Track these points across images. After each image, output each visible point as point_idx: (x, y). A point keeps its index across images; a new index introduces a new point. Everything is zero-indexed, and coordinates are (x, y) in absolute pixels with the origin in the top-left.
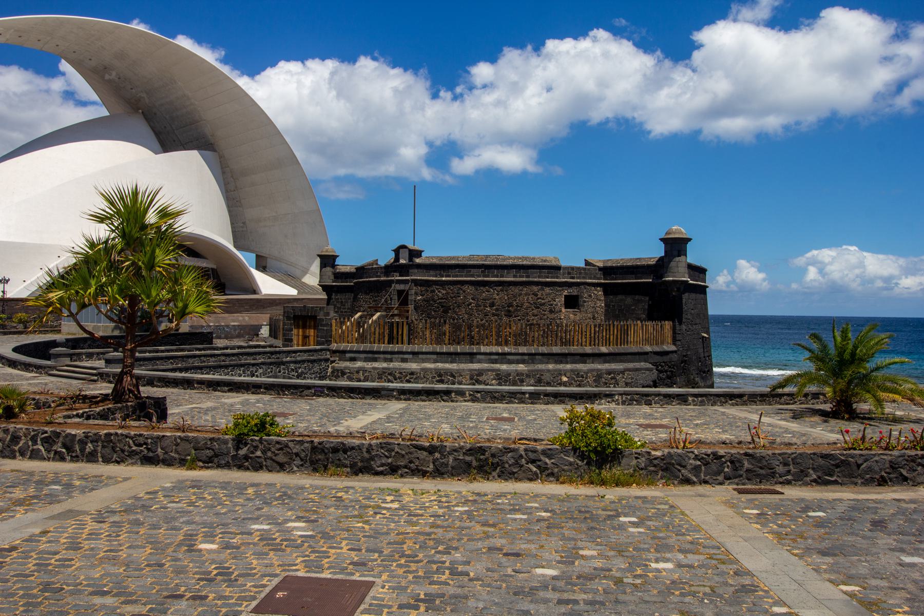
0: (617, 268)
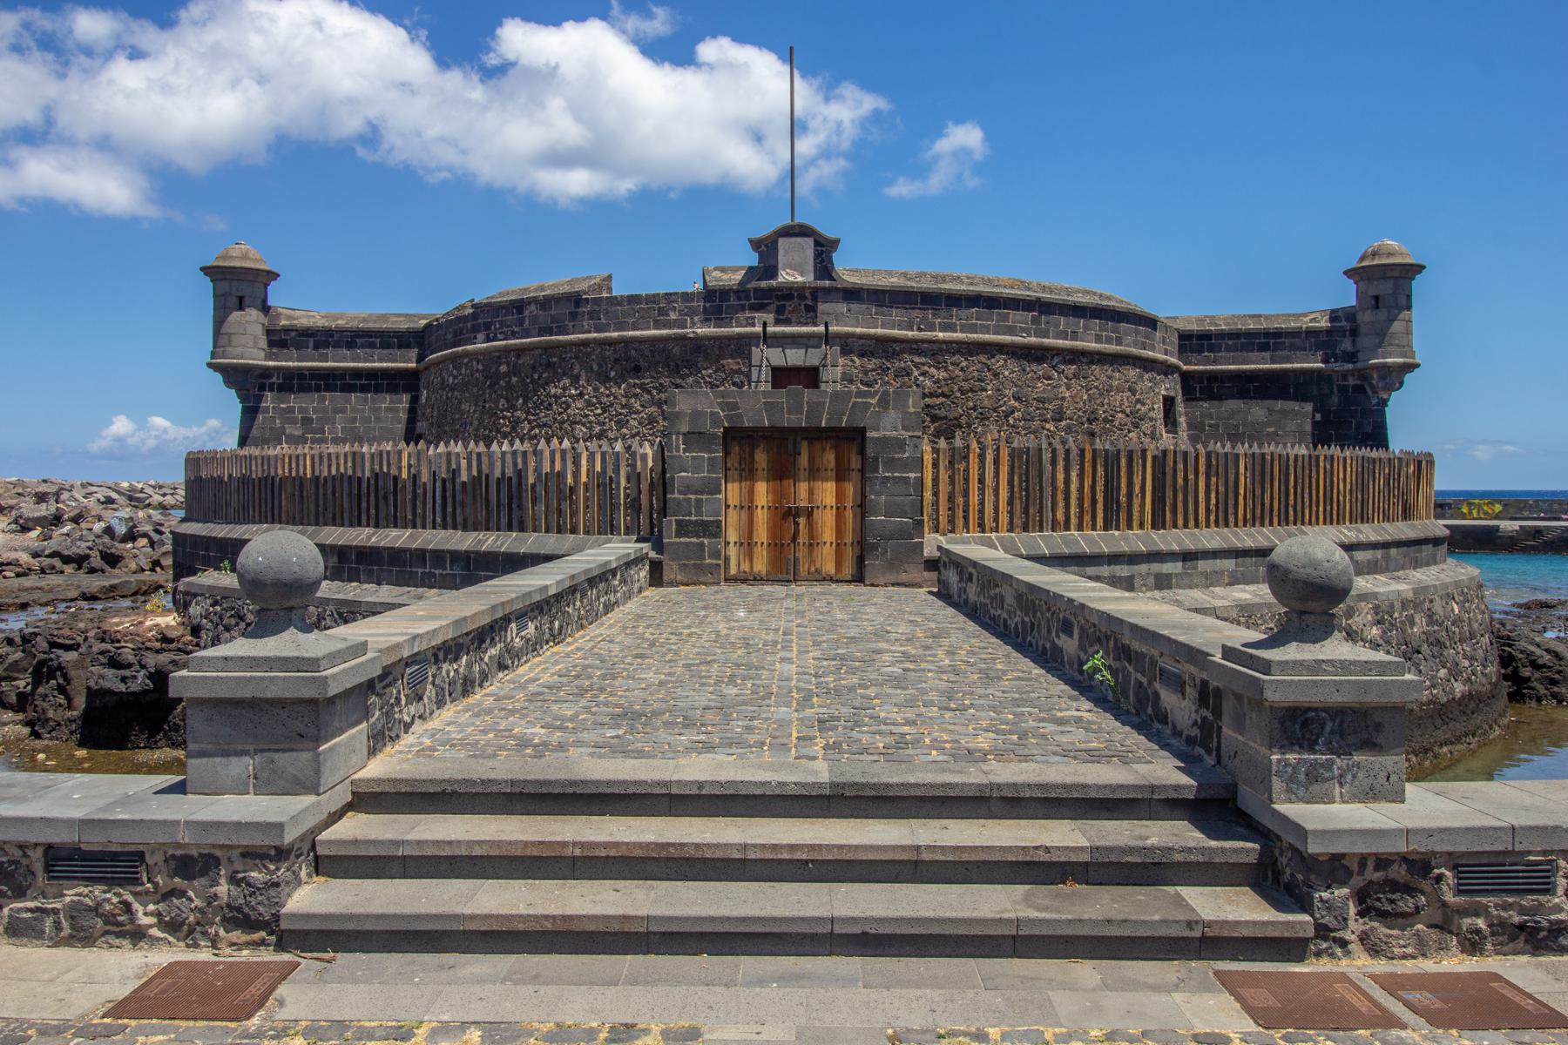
0: (1222, 335)
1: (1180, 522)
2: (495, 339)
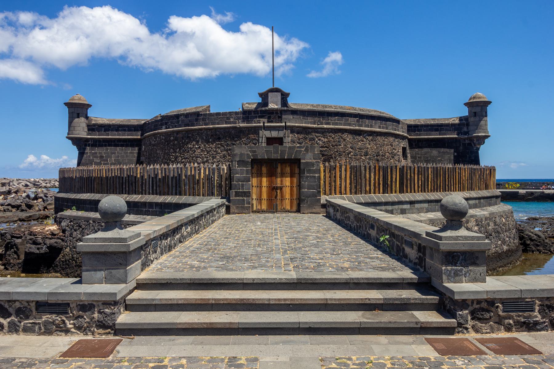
0: (422, 126)
1: (409, 191)
2: (169, 128)
